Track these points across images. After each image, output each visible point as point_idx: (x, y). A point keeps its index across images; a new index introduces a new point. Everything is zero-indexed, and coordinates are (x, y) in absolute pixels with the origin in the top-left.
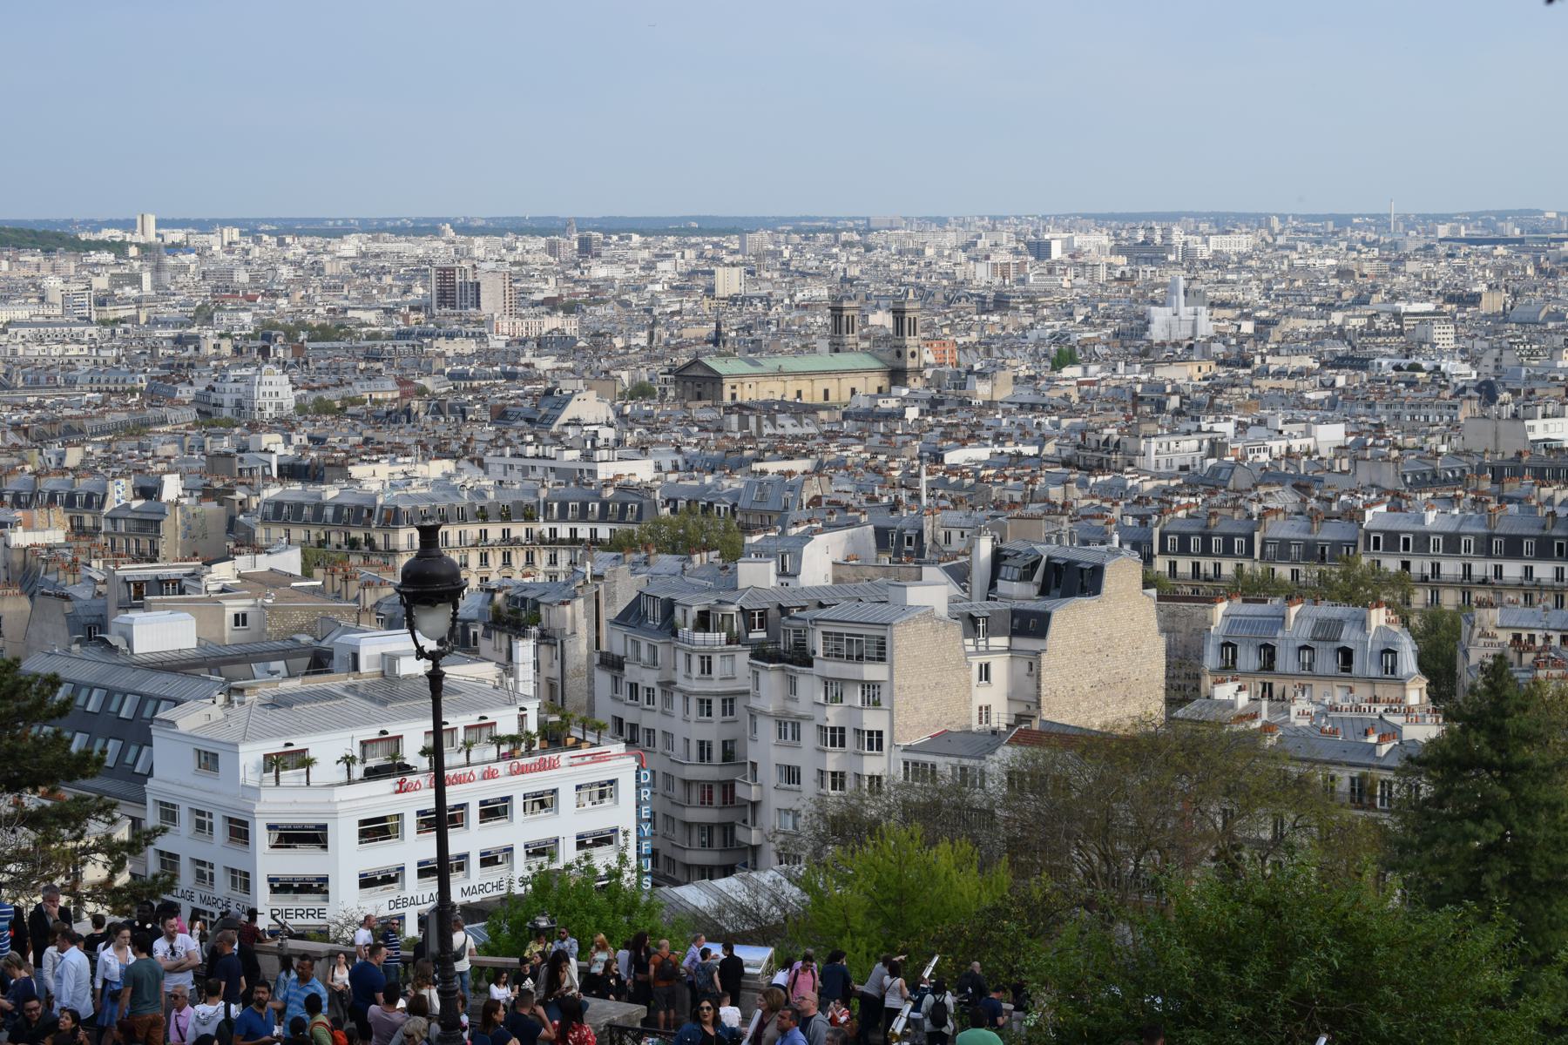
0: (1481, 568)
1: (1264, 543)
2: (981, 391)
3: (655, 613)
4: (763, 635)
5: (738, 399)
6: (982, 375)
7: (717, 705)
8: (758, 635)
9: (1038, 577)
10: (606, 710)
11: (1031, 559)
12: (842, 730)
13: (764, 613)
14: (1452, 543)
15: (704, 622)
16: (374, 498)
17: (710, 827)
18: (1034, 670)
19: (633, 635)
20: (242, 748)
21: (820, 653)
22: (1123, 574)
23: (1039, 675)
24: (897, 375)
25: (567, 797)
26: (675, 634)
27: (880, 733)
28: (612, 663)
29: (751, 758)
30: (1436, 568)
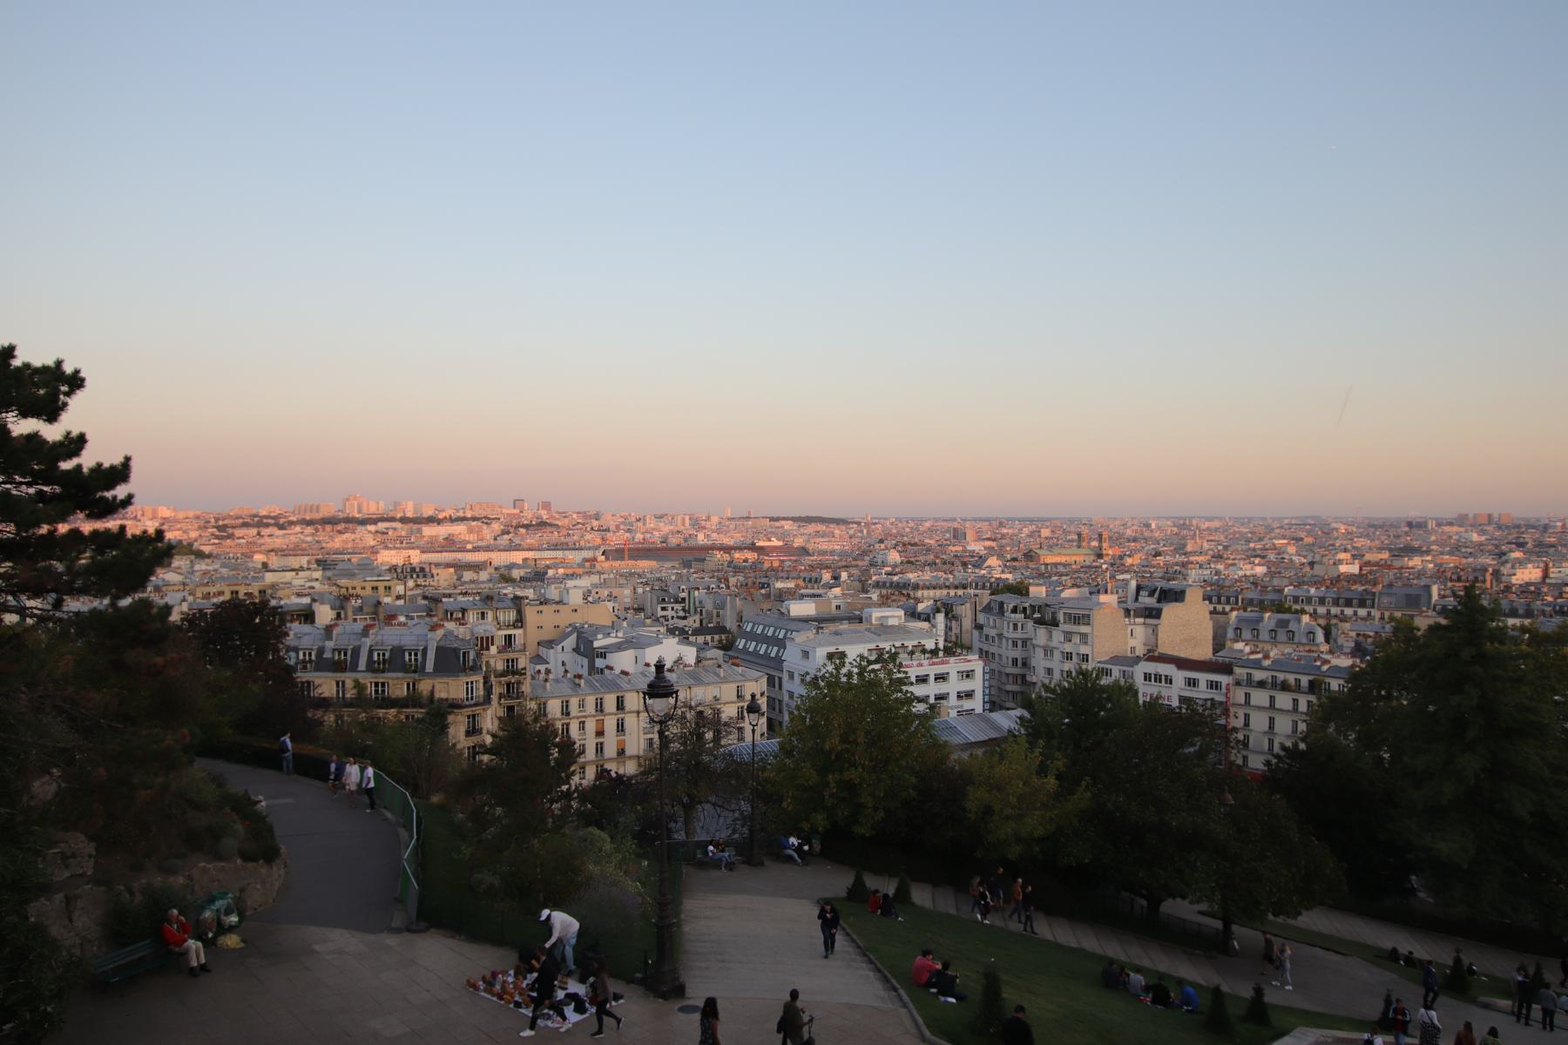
0: (1335, 610)
1: (1243, 600)
2: (1129, 561)
3: (996, 607)
4: (1039, 616)
6: (1129, 556)
7: (1020, 643)
8: (1037, 615)
9: (1156, 595)
10: (976, 645)
11: (1153, 588)
12: (1071, 653)
13: (1040, 607)
14: (1322, 601)
15: (1015, 610)
16: (910, 580)
17: (1017, 693)
18: (1155, 632)
20: (817, 649)
21: (1062, 621)
22: (1194, 596)
23: (1157, 635)
24: (1100, 556)
25: (953, 677)
26: (1003, 615)
27: (1087, 655)
28: (979, 627)
29: (1033, 664)
30: (1315, 611)
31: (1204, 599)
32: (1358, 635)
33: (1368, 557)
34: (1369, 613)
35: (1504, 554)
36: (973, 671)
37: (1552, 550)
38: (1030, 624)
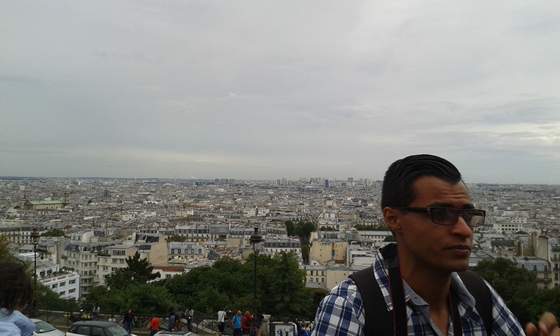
0: (195, 235)
5: (36, 209)
6: (81, 204)
7: (88, 264)
9: (146, 239)
15: (85, 250)
17: (87, 287)
19: (69, 252)
24: (65, 204)
26: (80, 252)
30: (187, 235)
31: (165, 240)
32: (208, 247)
33: (185, 201)
34: (207, 235)
35: (236, 199)
36: (75, 280)
37: (251, 197)
38: (93, 256)
